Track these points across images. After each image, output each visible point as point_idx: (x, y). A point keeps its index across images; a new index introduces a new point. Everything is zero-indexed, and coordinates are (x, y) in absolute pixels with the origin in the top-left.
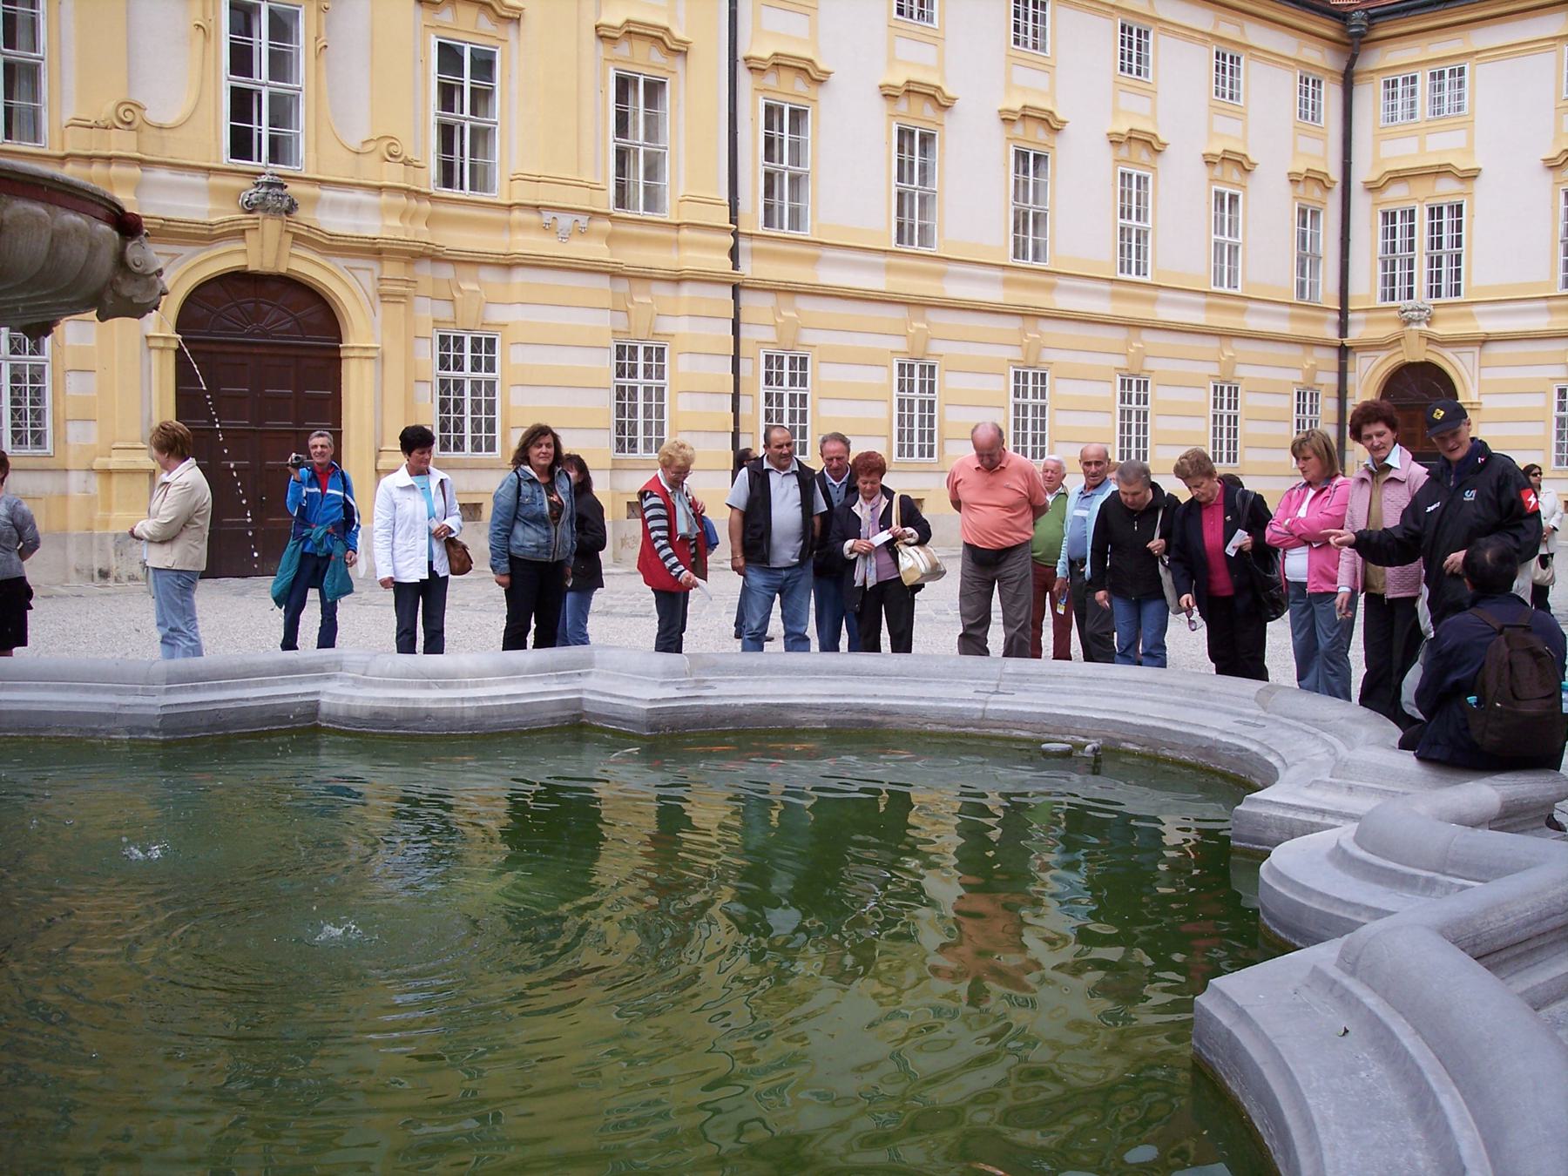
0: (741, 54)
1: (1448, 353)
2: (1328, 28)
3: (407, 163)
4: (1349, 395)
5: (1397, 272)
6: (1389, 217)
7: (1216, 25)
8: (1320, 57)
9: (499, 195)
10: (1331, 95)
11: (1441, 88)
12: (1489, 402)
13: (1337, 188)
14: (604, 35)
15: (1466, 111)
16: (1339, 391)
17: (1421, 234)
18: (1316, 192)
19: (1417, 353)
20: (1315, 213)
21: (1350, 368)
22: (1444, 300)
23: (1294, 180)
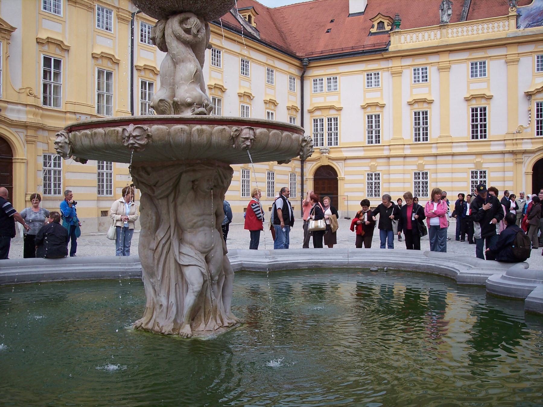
0: (135, 64)
1: (334, 162)
2: (297, 63)
3: (35, 97)
4: (304, 175)
5: (318, 138)
6: (315, 121)
7: (267, 61)
8: (295, 71)
9: (62, 108)
10: (298, 82)
11: (330, 83)
12: (347, 178)
13: (300, 111)
14: (94, 57)
15: (338, 90)
16: (301, 174)
17: (325, 126)
18: (294, 113)
19: (326, 163)
20: (294, 119)
21: (304, 167)
22: (333, 146)
23: (288, 109)
